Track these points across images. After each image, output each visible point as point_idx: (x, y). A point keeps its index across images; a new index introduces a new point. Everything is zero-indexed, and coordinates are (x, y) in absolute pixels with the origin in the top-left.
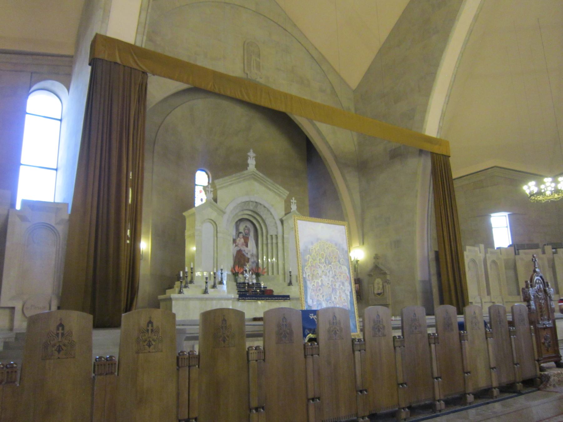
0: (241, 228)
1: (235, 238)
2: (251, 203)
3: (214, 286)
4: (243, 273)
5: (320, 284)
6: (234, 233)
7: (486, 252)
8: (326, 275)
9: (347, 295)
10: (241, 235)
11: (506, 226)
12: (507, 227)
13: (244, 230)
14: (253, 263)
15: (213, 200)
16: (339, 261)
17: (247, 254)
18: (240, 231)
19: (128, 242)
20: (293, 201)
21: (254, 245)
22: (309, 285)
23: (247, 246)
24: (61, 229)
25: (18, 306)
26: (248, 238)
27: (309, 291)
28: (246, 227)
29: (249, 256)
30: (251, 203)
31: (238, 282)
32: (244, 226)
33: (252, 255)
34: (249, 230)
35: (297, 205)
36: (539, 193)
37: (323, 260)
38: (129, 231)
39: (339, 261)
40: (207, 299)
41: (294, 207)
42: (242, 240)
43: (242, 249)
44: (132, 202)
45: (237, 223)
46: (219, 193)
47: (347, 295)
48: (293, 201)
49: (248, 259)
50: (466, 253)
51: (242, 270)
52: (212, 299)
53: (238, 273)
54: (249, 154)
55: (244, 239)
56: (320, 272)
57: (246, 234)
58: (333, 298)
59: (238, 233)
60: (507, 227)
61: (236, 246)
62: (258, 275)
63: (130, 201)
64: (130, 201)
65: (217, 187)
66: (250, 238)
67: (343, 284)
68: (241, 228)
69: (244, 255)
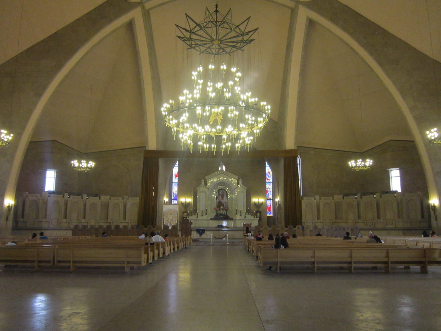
0: (221, 192)
1: (217, 196)
2: (222, 183)
3: (202, 216)
4: (219, 210)
5: (168, 219)
6: (217, 194)
7: (320, 199)
8: (170, 217)
9: (176, 222)
10: (220, 195)
11: (392, 178)
12: (391, 177)
13: (222, 193)
14: (226, 205)
15: (204, 184)
16: (175, 214)
17: (223, 202)
18: (220, 194)
19: (153, 206)
20: (240, 180)
21: (227, 199)
22: (165, 219)
23: (223, 199)
24: (138, 204)
25: (129, 222)
26: (223, 196)
27: (165, 221)
28: (223, 192)
29: (224, 203)
30: (222, 183)
31: (218, 213)
32: (222, 191)
33: (225, 203)
34: (224, 193)
35: (242, 182)
36: (356, 166)
37: (170, 214)
38: (153, 203)
39: (175, 214)
40: (197, 220)
41: (240, 183)
42: (221, 197)
43: (221, 200)
44: (154, 195)
45: (218, 190)
46: (207, 181)
47: (176, 222)
48: (240, 180)
49: (224, 204)
50: (303, 201)
51: (219, 209)
52: (199, 220)
53: (217, 210)
54: (220, 164)
55: (222, 197)
56: (168, 216)
57: (222, 195)
58: (171, 222)
59: (219, 195)
60: (391, 177)
61: (218, 199)
62: (226, 210)
63: (153, 195)
64: (153, 195)
65: (206, 179)
66: (224, 196)
67: (175, 219)
68: (221, 192)
69: (222, 203)
